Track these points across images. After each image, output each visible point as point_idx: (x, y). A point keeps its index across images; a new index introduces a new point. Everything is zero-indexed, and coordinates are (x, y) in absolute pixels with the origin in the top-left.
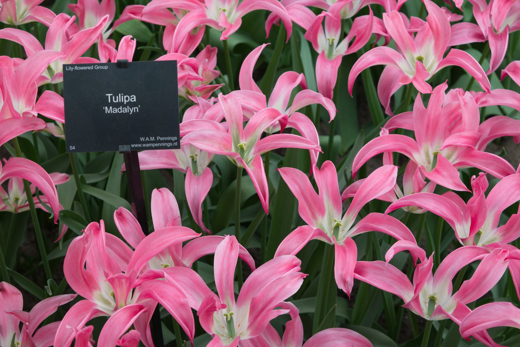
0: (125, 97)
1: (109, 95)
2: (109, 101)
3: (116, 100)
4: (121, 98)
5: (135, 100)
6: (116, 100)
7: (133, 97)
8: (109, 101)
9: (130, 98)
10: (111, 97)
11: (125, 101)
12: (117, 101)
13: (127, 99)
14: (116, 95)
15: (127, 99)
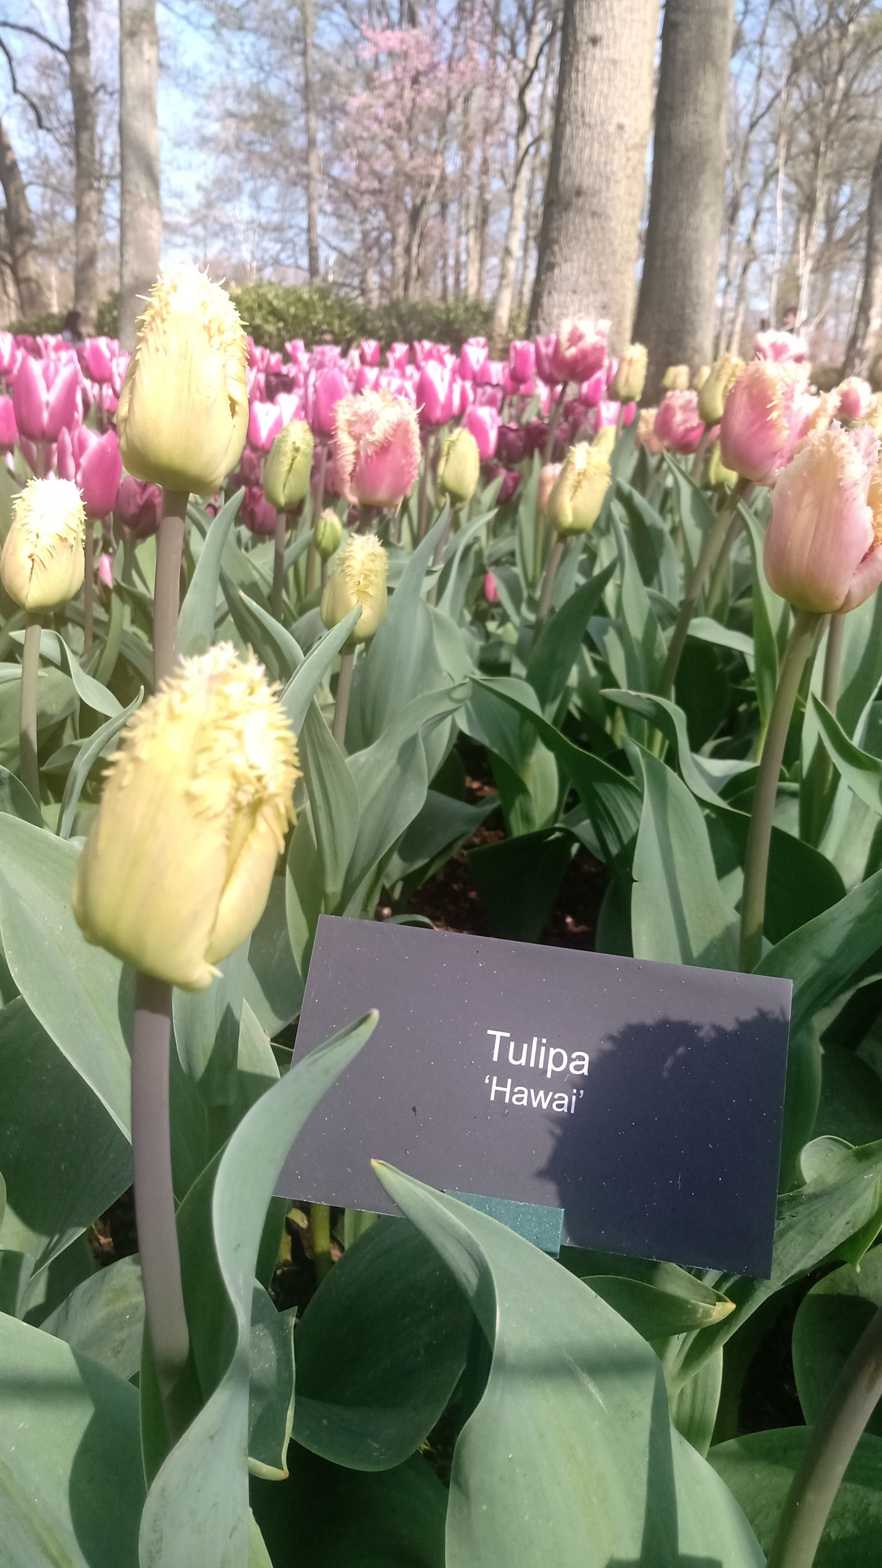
0: (552, 1052)
1: (499, 1034)
2: (495, 1058)
3: (517, 1057)
4: (539, 1054)
5: (585, 1071)
6: (517, 1057)
7: (582, 1059)
8: (495, 1058)
9: (570, 1060)
10: (504, 1042)
11: (551, 1066)
12: (523, 1061)
13: (558, 1060)
14: (521, 1037)
15: (558, 1060)
